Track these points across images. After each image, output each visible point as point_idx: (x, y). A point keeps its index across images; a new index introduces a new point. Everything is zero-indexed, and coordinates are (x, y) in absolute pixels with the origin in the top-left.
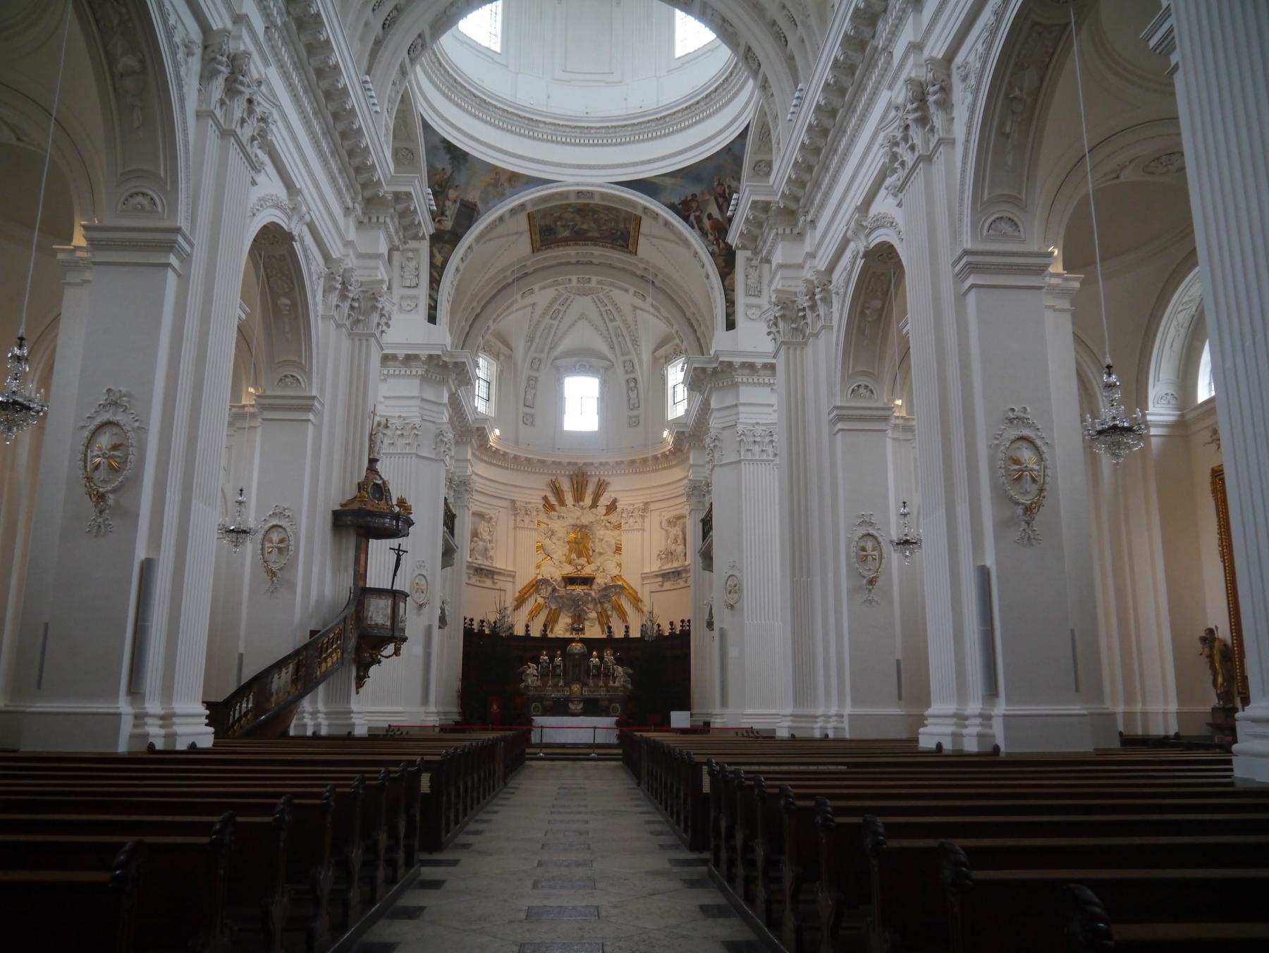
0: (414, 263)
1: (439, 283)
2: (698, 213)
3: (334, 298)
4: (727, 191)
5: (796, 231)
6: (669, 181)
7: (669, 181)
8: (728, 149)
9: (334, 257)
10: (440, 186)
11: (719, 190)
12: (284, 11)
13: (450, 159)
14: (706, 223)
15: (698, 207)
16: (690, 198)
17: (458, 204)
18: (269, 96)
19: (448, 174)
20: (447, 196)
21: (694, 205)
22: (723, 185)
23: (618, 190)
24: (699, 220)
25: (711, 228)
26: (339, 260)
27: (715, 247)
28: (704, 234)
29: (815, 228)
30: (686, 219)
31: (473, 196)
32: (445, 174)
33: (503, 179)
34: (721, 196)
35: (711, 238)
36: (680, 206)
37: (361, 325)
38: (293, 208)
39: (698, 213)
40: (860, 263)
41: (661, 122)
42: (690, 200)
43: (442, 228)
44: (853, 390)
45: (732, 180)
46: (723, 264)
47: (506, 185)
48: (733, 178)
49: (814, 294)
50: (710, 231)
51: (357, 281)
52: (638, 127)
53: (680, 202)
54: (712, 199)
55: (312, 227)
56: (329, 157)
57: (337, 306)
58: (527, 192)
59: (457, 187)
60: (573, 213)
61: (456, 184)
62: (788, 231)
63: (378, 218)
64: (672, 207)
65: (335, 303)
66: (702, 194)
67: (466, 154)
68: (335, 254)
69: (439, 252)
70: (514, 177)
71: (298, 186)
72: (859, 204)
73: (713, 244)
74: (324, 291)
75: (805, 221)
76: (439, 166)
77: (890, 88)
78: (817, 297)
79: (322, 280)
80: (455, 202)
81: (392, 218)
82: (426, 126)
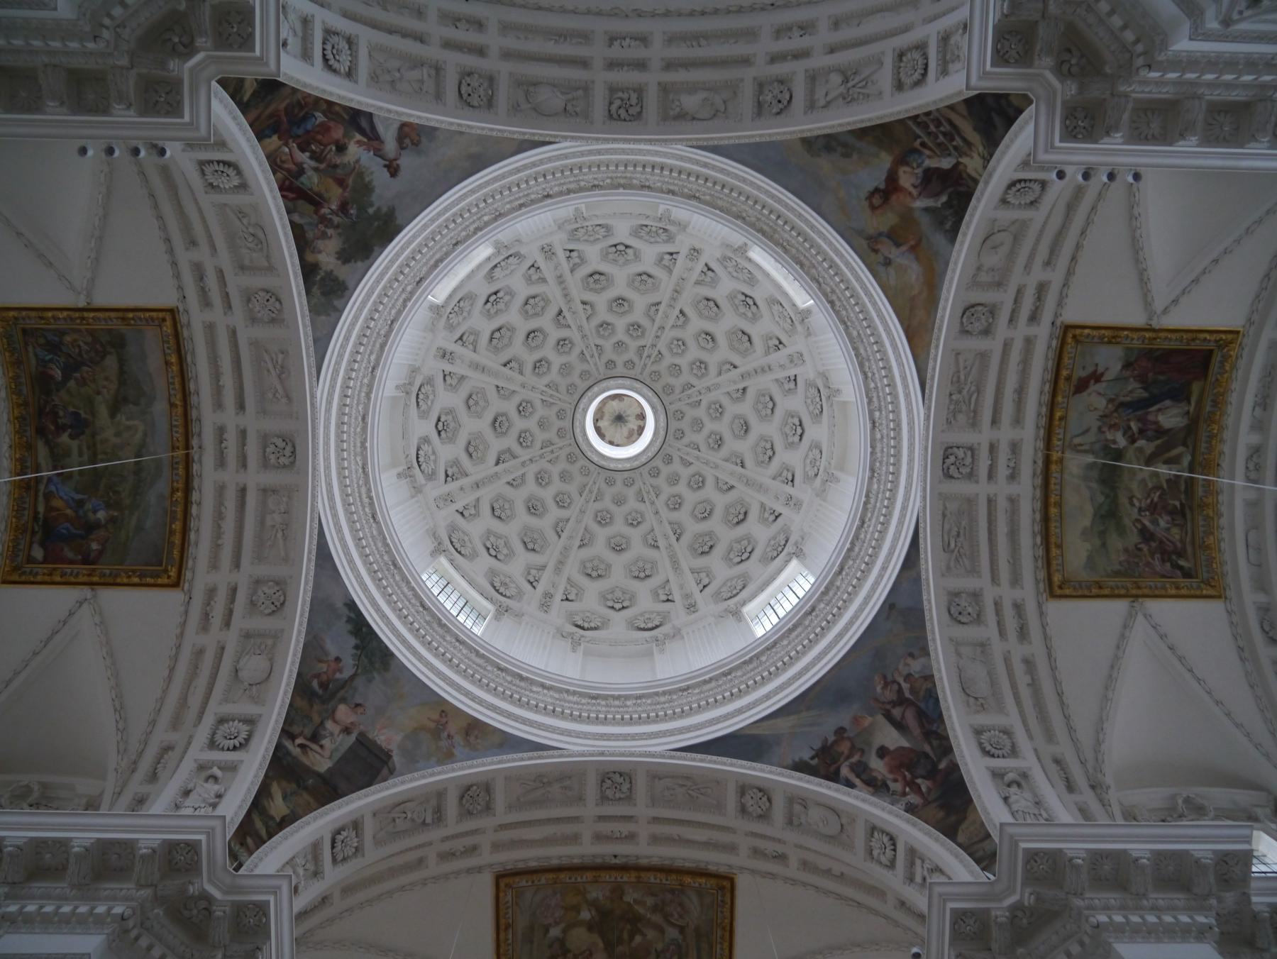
0: (213, 788)
1: (261, 842)
2: (855, 759)
4: (905, 686)
6: (784, 724)
7: (784, 724)
8: (889, 606)
10: (324, 685)
11: (890, 695)
13: (356, 647)
14: (878, 766)
15: (853, 747)
16: (831, 739)
17: (352, 739)
19: (347, 674)
20: (334, 711)
21: (844, 747)
22: (894, 682)
23: (679, 758)
24: (861, 770)
25: (891, 772)
27: (914, 799)
28: (877, 786)
30: (833, 777)
31: (388, 738)
32: (340, 671)
33: (452, 728)
34: (894, 704)
35: (896, 787)
36: (815, 762)
39: (855, 759)
41: (754, 664)
42: (835, 742)
43: (304, 760)
45: (910, 661)
46: (941, 814)
47: (458, 739)
48: (911, 655)
50: (891, 776)
52: (713, 684)
53: (813, 753)
54: (880, 718)
58: (500, 758)
59: (357, 705)
60: (590, 927)
61: (359, 701)
64: (800, 767)
66: (856, 720)
67: (386, 656)
69: (284, 798)
70: (474, 728)
73: (904, 794)
76: (332, 649)
80: (347, 730)
82: (324, 555)
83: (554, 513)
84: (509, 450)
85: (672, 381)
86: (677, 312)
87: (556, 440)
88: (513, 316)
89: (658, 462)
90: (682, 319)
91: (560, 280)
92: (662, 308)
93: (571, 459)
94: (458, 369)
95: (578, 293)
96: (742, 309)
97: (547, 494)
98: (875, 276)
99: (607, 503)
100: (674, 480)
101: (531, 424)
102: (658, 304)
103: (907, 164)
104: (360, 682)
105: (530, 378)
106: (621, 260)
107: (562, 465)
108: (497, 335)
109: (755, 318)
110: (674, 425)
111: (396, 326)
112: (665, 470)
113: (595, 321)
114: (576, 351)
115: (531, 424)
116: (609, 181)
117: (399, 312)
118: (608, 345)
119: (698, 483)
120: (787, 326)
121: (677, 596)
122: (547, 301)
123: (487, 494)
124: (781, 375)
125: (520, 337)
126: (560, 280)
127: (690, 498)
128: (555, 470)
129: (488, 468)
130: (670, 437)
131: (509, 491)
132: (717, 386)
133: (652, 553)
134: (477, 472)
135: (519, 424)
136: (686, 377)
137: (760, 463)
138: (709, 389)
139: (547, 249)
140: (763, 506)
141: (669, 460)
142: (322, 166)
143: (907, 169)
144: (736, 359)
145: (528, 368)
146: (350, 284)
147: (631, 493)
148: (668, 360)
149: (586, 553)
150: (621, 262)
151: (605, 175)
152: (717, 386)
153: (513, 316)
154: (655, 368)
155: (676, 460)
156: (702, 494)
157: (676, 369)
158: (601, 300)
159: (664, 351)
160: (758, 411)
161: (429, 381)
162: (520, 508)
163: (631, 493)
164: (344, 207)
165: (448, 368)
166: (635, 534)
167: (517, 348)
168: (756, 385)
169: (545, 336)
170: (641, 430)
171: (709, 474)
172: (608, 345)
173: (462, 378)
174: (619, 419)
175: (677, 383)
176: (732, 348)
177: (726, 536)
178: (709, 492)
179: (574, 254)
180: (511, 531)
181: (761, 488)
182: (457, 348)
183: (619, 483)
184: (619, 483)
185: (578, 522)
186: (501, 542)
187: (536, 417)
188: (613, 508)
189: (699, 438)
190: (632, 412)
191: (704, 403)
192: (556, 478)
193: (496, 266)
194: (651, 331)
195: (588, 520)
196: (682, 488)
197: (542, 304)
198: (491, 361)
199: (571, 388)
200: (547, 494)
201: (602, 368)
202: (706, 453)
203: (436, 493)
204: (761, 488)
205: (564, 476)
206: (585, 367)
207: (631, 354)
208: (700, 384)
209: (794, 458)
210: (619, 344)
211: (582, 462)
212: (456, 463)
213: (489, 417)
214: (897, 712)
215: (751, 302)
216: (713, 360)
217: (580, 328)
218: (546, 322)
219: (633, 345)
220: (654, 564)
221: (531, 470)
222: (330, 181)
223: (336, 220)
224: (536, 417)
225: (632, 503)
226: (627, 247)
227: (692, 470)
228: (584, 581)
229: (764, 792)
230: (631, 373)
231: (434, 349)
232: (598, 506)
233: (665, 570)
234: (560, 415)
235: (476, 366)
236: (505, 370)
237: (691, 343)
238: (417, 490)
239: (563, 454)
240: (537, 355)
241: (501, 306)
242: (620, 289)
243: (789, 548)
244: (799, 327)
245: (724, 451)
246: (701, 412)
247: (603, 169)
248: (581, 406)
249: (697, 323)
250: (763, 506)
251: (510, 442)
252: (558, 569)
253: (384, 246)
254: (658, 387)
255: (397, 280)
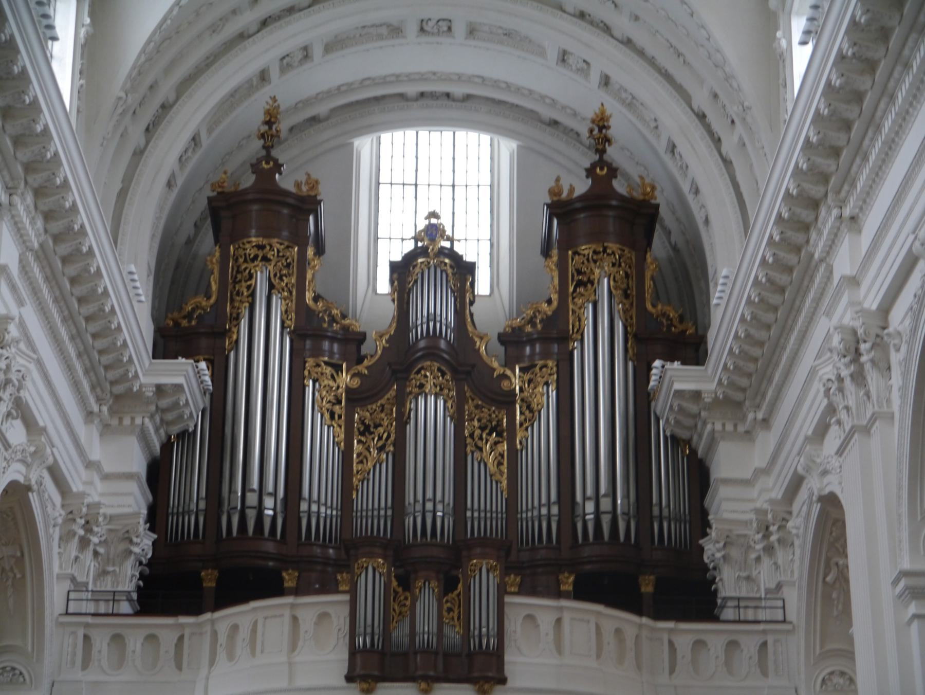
3: (73, 548)
5: (741, 429)
9: (75, 489)
12: (42, 230)
18: (28, 352)
26: (83, 495)
29: (859, 231)
37: (109, 578)
38: (35, 452)
40: (816, 508)
44: (823, 680)
49: (858, 353)
51: (105, 516)
55: (54, 472)
56: (59, 324)
57: (77, 558)
62: (729, 427)
63: (133, 419)
65: (74, 553)
68: (76, 486)
71: (41, 424)
72: (810, 432)
74: (61, 538)
75: (755, 419)
77: (829, 314)
78: (864, 359)
79: (57, 529)
81: (152, 417)
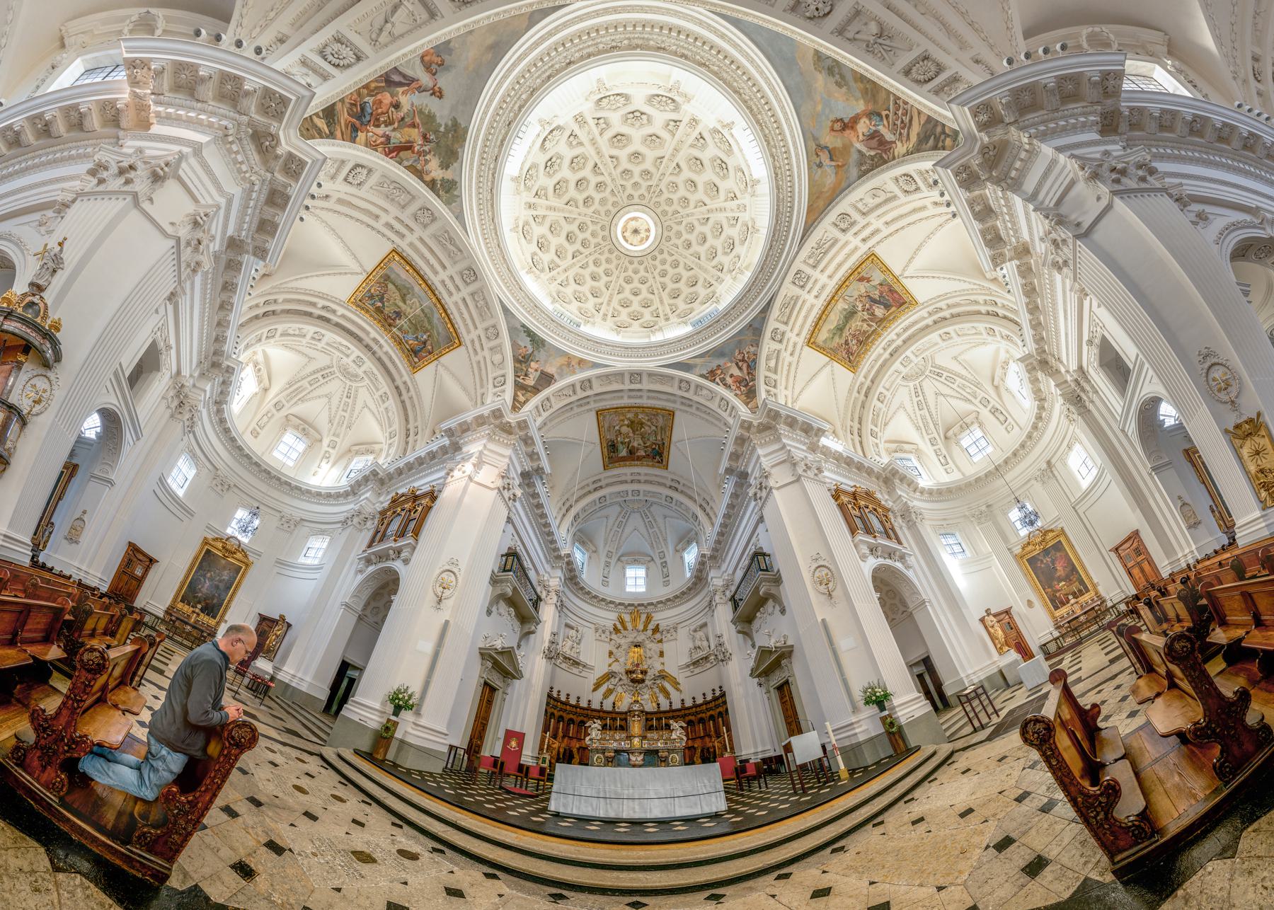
11: (740, 357)
21: (719, 372)
24: (723, 380)
30: (713, 381)
31: (551, 370)
64: (702, 376)
76: (522, 344)
80: (536, 370)
83: (605, 279)
84: (578, 251)
85: (667, 208)
86: (674, 165)
87: (602, 242)
88: (565, 172)
89: (656, 253)
90: (678, 170)
91: (593, 142)
92: (665, 160)
93: (610, 252)
94: (540, 212)
95: (607, 150)
96: (718, 170)
97: (600, 270)
98: (809, 169)
99: (630, 273)
100: (664, 262)
101: (587, 235)
102: (663, 157)
103: (870, 119)
104: (535, 353)
105: (582, 209)
106: (638, 124)
107: (606, 255)
108: (558, 187)
109: (724, 177)
110: (666, 234)
111: (494, 191)
112: (659, 257)
113: (620, 169)
114: (609, 190)
115: (587, 235)
116: (626, 42)
117: (493, 183)
118: (628, 184)
119: (676, 265)
120: (742, 187)
121: (661, 315)
122: (586, 159)
123: (571, 274)
124: (730, 215)
125: (572, 185)
126: (593, 142)
127: (671, 272)
128: (603, 258)
129: (569, 261)
130: (663, 240)
131: (581, 271)
132: (692, 214)
133: (651, 296)
134: (564, 264)
135: (581, 236)
136: (676, 207)
137: (708, 259)
138: (688, 215)
139: (580, 119)
140: (705, 279)
141: (662, 252)
142: (396, 125)
143: (868, 122)
144: (707, 201)
145: (581, 203)
146: (457, 179)
147: (642, 268)
148: (666, 195)
149: (621, 296)
150: (637, 126)
151: (623, 36)
152: (692, 214)
153: (565, 172)
154: (657, 200)
155: (666, 252)
156: (677, 271)
157: (670, 201)
158: (623, 154)
159: (664, 190)
160: (713, 232)
161: (526, 223)
162: (588, 279)
163: (642, 268)
164: (425, 137)
165: (535, 213)
166: (644, 288)
167: (572, 192)
168: (714, 217)
169: (588, 182)
170: (648, 237)
171: (682, 261)
172: (628, 184)
173: (544, 217)
174: (636, 231)
175: (670, 210)
176: (706, 193)
177: (686, 291)
178: (681, 269)
179: (601, 121)
180: (585, 289)
181: (706, 271)
182: (536, 200)
183: (636, 263)
184: (636, 263)
185: (616, 282)
186: (581, 295)
187: (589, 231)
188: (633, 275)
189: (679, 242)
190: (642, 228)
191: (684, 223)
192: (604, 262)
193: (545, 140)
194: (656, 176)
195: (621, 281)
196: (667, 267)
197: (583, 161)
198: (558, 203)
199: (608, 212)
200: (600, 270)
201: (625, 200)
202: (681, 250)
203: (547, 277)
204: (706, 271)
205: (608, 261)
206: (615, 199)
207: (643, 191)
208: (683, 212)
209: (726, 260)
210: (636, 184)
211: (616, 253)
212: (553, 261)
213: (564, 235)
214: (740, 364)
215: (724, 166)
216: (693, 198)
217: (610, 174)
218: (586, 172)
219: (644, 184)
220: (652, 301)
221: (591, 259)
222: (406, 129)
223: (426, 148)
224: (589, 231)
225: (642, 273)
226: (642, 114)
227: (674, 258)
228: (620, 309)
229: (688, 382)
230: (643, 202)
231: (523, 206)
232: (626, 274)
233: (657, 304)
234: (603, 228)
235: (550, 208)
236: (568, 207)
237: (681, 186)
238: (538, 277)
239: (606, 249)
240: (585, 195)
241: (556, 167)
242: (636, 146)
243: (714, 299)
244: (749, 189)
245: (691, 251)
246: (682, 228)
247: (620, 29)
248: (614, 222)
249: (687, 174)
250: (705, 279)
251: (578, 246)
252: (608, 304)
253: (463, 146)
254: (658, 211)
255: (482, 164)
